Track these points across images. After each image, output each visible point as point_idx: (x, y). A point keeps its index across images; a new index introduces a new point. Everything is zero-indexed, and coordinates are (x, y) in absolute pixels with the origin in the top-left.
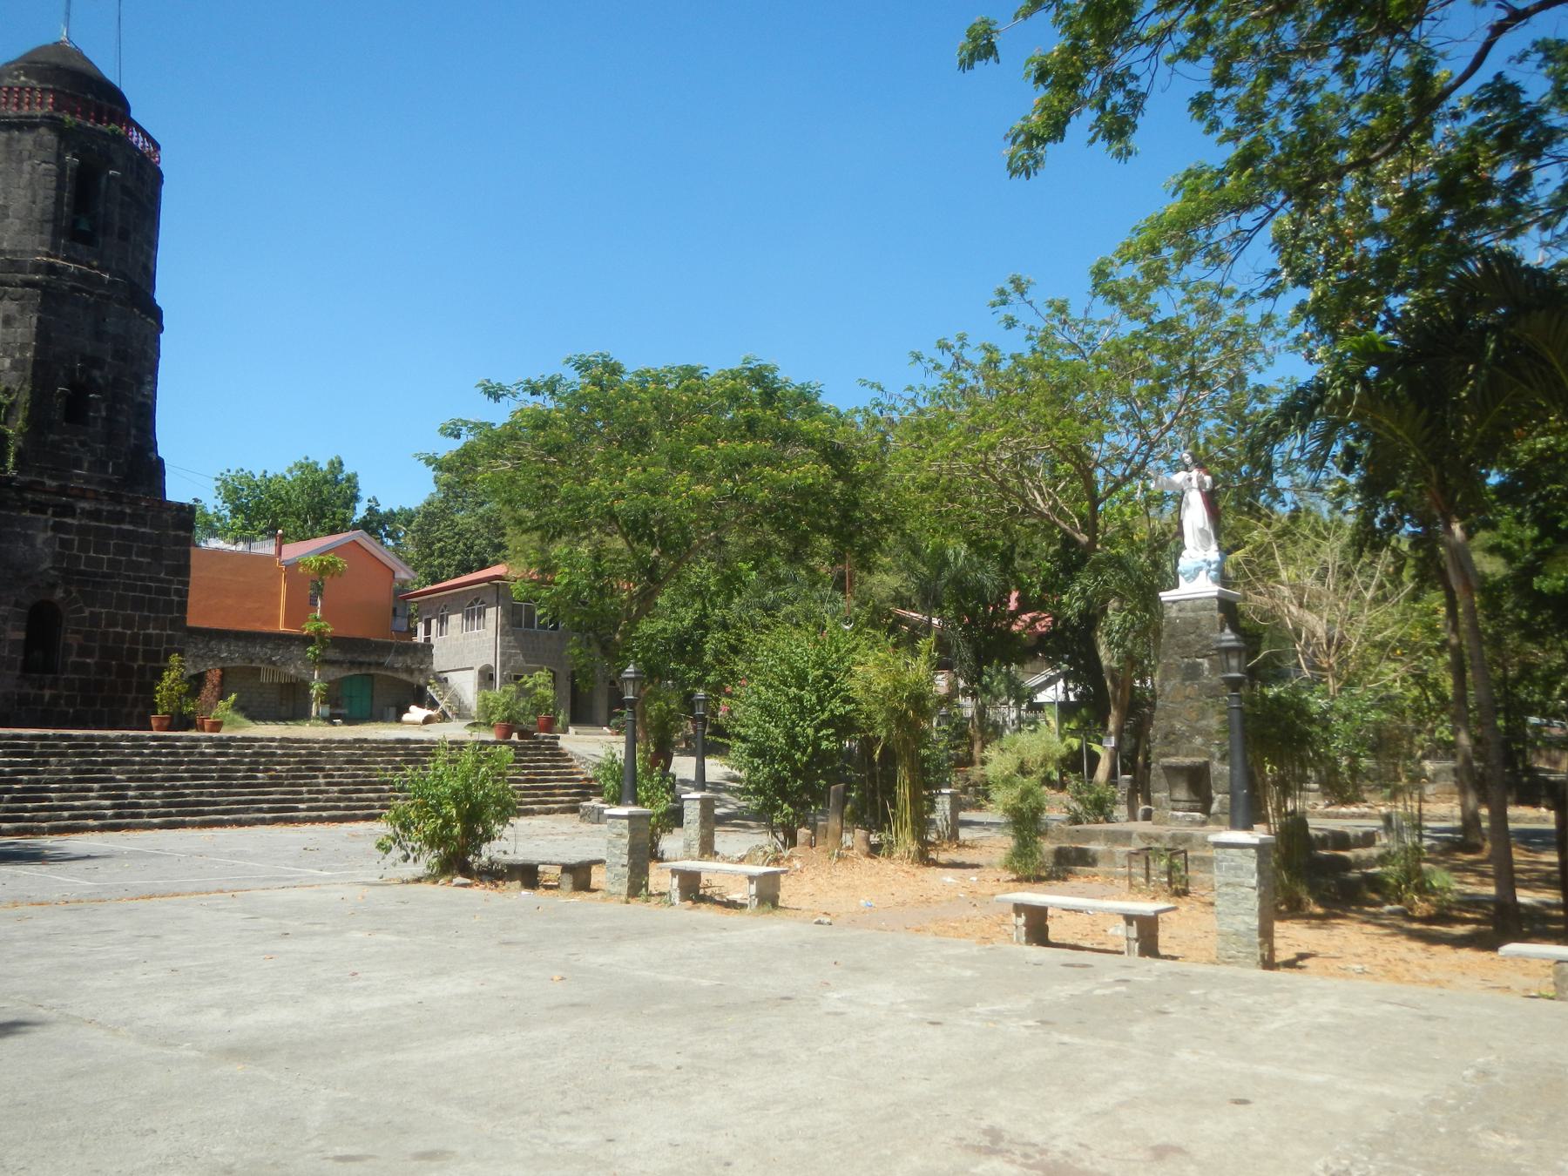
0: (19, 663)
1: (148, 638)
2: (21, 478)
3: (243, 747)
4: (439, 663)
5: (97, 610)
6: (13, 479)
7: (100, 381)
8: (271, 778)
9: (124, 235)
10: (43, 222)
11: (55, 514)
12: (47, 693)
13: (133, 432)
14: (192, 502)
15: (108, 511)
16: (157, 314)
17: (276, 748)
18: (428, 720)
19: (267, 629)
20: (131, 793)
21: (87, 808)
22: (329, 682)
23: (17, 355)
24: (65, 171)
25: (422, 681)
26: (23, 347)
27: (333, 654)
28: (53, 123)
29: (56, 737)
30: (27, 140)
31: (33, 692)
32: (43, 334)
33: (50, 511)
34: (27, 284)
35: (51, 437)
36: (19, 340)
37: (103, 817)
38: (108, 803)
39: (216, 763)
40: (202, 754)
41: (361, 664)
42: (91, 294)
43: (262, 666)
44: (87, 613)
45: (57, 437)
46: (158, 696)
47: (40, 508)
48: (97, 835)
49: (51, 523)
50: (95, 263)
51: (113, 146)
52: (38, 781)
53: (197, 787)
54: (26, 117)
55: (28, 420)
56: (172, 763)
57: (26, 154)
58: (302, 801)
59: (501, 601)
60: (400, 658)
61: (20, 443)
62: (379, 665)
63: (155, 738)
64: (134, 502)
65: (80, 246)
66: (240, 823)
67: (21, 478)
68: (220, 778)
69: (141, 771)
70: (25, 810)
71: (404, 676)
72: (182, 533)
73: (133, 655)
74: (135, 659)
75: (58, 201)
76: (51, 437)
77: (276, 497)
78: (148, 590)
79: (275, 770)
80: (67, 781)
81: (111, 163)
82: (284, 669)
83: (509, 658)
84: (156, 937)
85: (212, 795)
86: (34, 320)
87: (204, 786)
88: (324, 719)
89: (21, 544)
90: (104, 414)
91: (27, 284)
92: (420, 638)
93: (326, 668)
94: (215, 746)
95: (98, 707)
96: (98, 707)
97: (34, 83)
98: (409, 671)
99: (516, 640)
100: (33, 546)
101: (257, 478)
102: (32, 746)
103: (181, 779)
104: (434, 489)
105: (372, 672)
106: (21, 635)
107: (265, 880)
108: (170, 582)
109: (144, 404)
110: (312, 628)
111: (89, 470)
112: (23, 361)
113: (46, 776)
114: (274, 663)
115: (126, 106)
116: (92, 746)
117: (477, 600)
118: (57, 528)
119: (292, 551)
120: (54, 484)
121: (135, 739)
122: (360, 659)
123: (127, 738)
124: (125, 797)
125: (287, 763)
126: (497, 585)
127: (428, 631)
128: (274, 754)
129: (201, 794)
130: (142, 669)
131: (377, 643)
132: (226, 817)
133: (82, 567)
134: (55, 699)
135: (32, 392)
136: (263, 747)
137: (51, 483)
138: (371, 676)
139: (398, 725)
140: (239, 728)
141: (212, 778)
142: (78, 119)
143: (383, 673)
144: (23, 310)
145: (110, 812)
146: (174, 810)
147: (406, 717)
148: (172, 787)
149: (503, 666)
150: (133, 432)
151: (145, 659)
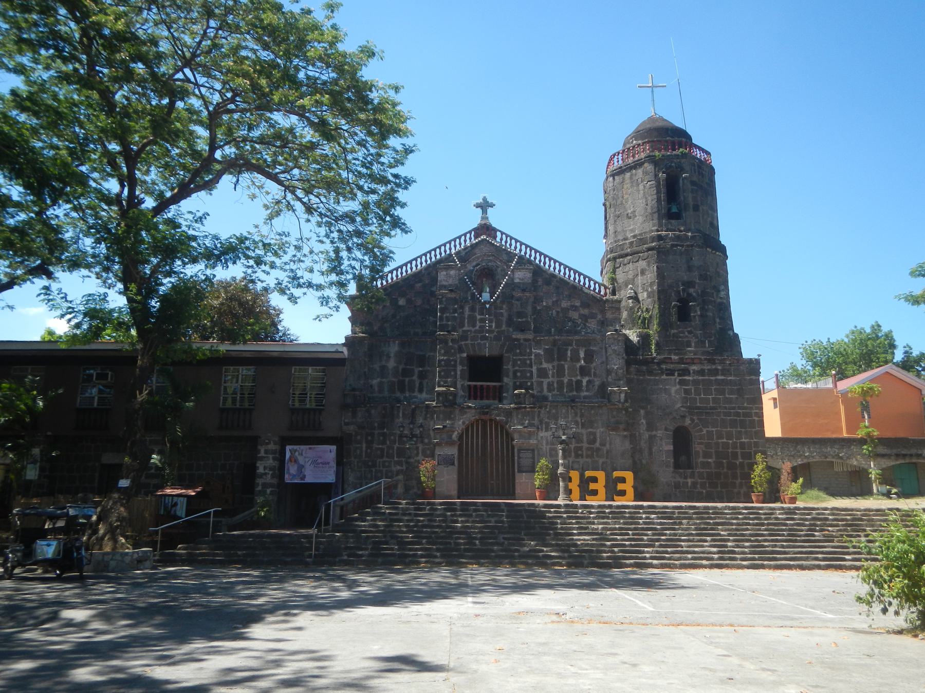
0: (672, 465)
1: (742, 444)
2: (659, 357)
3: (804, 514)
5: (710, 429)
6: (654, 358)
7: (694, 294)
8: (824, 536)
9: (696, 208)
10: (652, 214)
11: (679, 375)
12: (689, 481)
13: (718, 320)
14: (757, 357)
15: (708, 370)
16: (723, 249)
17: (829, 514)
19: (834, 436)
20: (729, 544)
21: (703, 552)
22: (882, 470)
23: (650, 290)
24: (660, 184)
26: (651, 284)
27: (881, 450)
28: (651, 159)
29: (687, 507)
30: (640, 172)
31: (681, 480)
32: (661, 275)
33: (676, 374)
34: (649, 249)
35: (673, 331)
36: (649, 281)
37: (712, 559)
38: (715, 550)
39: (786, 525)
40: (777, 519)
41: (904, 456)
42: (682, 246)
44: (705, 432)
45: (676, 331)
46: (753, 481)
47: (671, 373)
48: (707, 570)
49: (678, 380)
50: (682, 229)
51: (683, 161)
52: (675, 535)
53: (772, 541)
54: (638, 161)
55: (659, 324)
56: (757, 524)
57: (640, 180)
58: (848, 554)
61: (657, 338)
63: (746, 508)
64: (722, 362)
65: (673, 221)
66: (802, 568)
67: (659, 357)
68: (789, 535)
69: (737, 530)
70: (667, 552)
72: (754, 377)
73: (735, 455)
74: (737, 458)
75: (659, 200)
76: (673, 331)
77: (837, 353)
78: (738, 414)
79: (828, 531)
80: (692, 535)
81: (683, 170)
84: (634, 665)
85: (783, 547)
86: (655, 268)
87: (777, 541)
88: (883, 495)
89: (664, 395)
90: (699, 313)
91: (649, 249)
93: (879, 459)
94: (786, 513)
95: (719, 489)
96: (719, 489)
97: (640, 142)
100: (670, 395)
101: (825, 344)
102: (673, 513)
103: (762, 535)
105: (914, 461)
106: (671, 447)
107: (775, 618)
108: (751, 408)
109: (721, 304)
110: (863, 433)
111: (695, 347)
112: (653, 292)
113: (680, 532)
114: (841, 458)
115: (689, 138)
116: (708, 513)
118: (682, 383)
119: (843, 385)
120: (676, 358)
121: (734, 508)
122: (903, 452)
123: (729, 508)
124: (726, 546)
125: (837, 526)
128: (827, 519)
129: (775, 546)
130: (742, 464)
131: (913, 440)
132: (792, 563)
133: (698, 405)
134: (694, 485)
135: (659, 308)
136: (818, 514)
137: (675, 357)
140: (822, 501)
141: (783, 535)
142: (663, 152)
144: (649, 265)
145: (716, 556)
146: (756, 556)
148: (757, 541)
150: (718, 320)
151: (742, 458)
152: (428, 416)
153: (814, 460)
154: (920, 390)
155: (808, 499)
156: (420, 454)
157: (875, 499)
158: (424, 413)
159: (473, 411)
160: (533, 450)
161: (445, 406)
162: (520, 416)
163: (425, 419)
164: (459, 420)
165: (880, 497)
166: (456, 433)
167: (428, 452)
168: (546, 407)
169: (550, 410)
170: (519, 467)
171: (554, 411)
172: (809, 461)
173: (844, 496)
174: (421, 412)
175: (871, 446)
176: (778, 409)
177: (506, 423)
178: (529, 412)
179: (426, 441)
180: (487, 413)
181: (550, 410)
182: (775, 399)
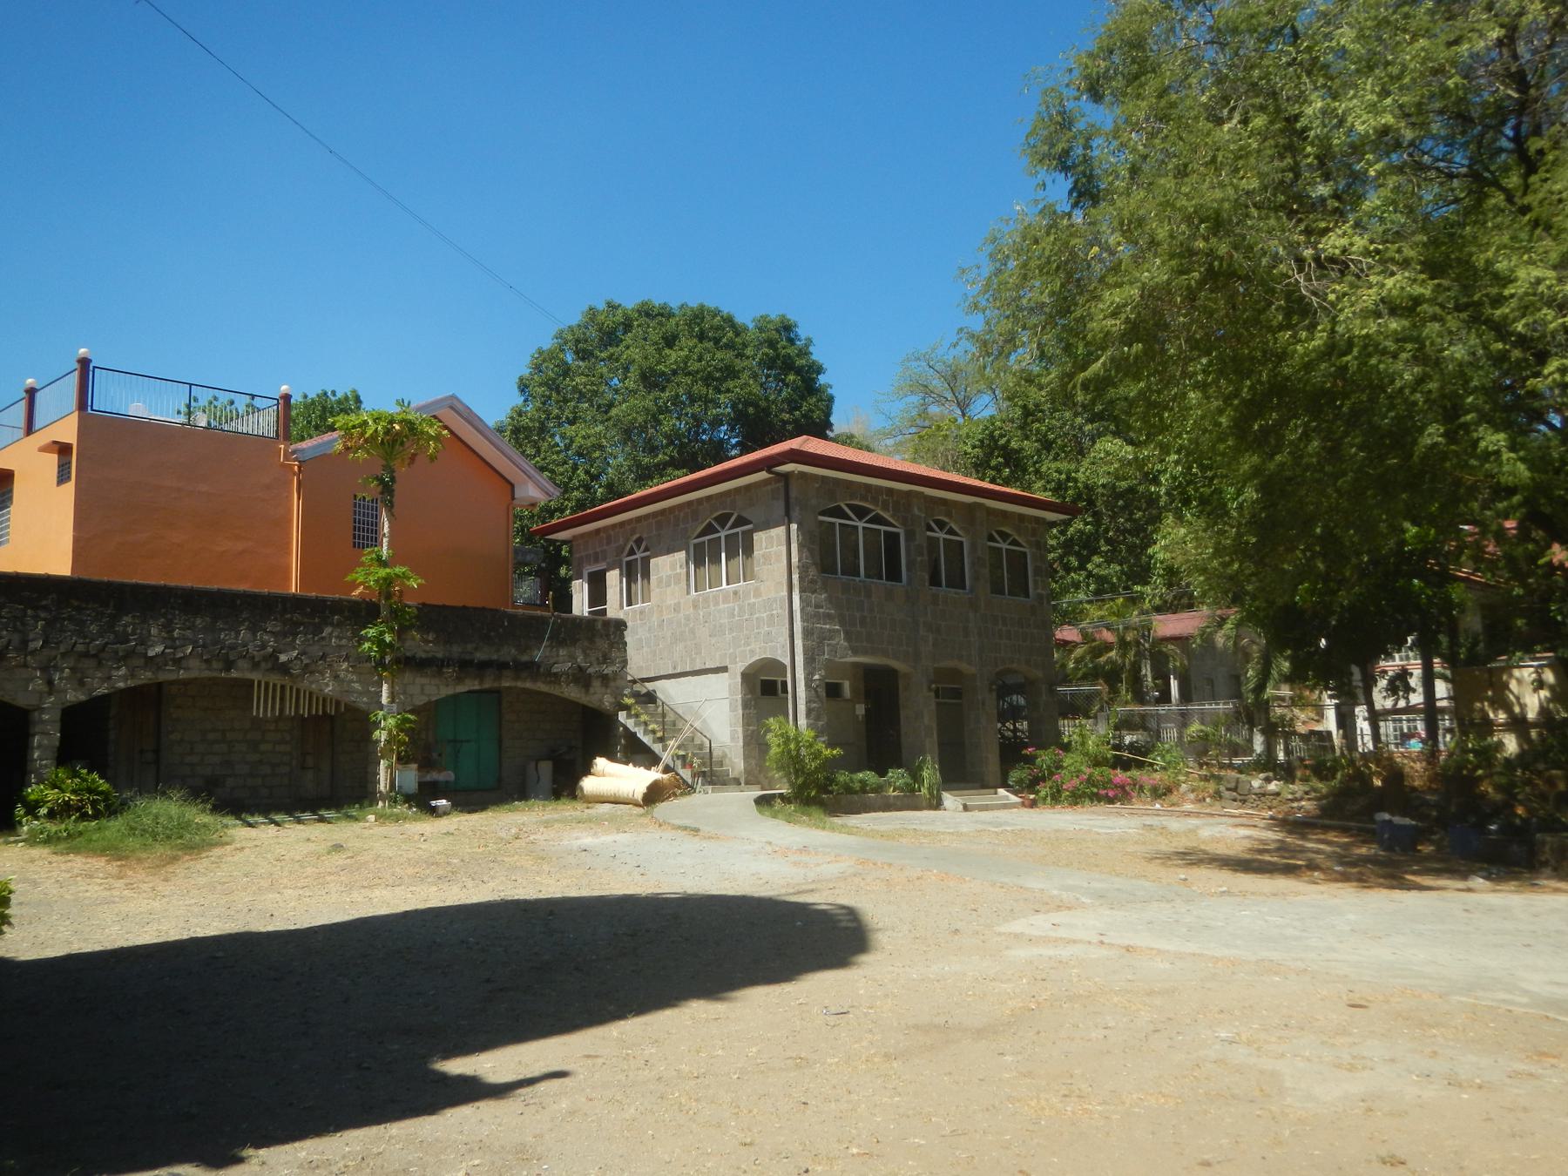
4: (639, 659)
18: (654, 795)
25: (608, 702)
27: (419, 644)
41: (484, 666)
43: (255, 676)
59: (796, 513)
60: (562, 652)
62: (531, 668)
71: (572, 692)
82: (307, 684)
83: (822, 639)
88: (409, 799)
92: (581, 604)
93: (408, 676)
98: (582, 678)
99: (830, 599)
104: (519, 400)
114: (284, 669)
117: (723, 520)
122: (480, 656)
126: (786, 477)
127: (598, 595)
138: (497, 692)
139: (566, 810)
143: (528, 685)
147: (589, 784)
149: (810, 660)
153: (182, 674)
154: (512, 486)
155: (131, 842)
157: (381, 817)
165: (400, 809)
172: (163, 677)
173: (280, 808)
175: (391, 630)
176: (70, 487)
182: (63, 450)
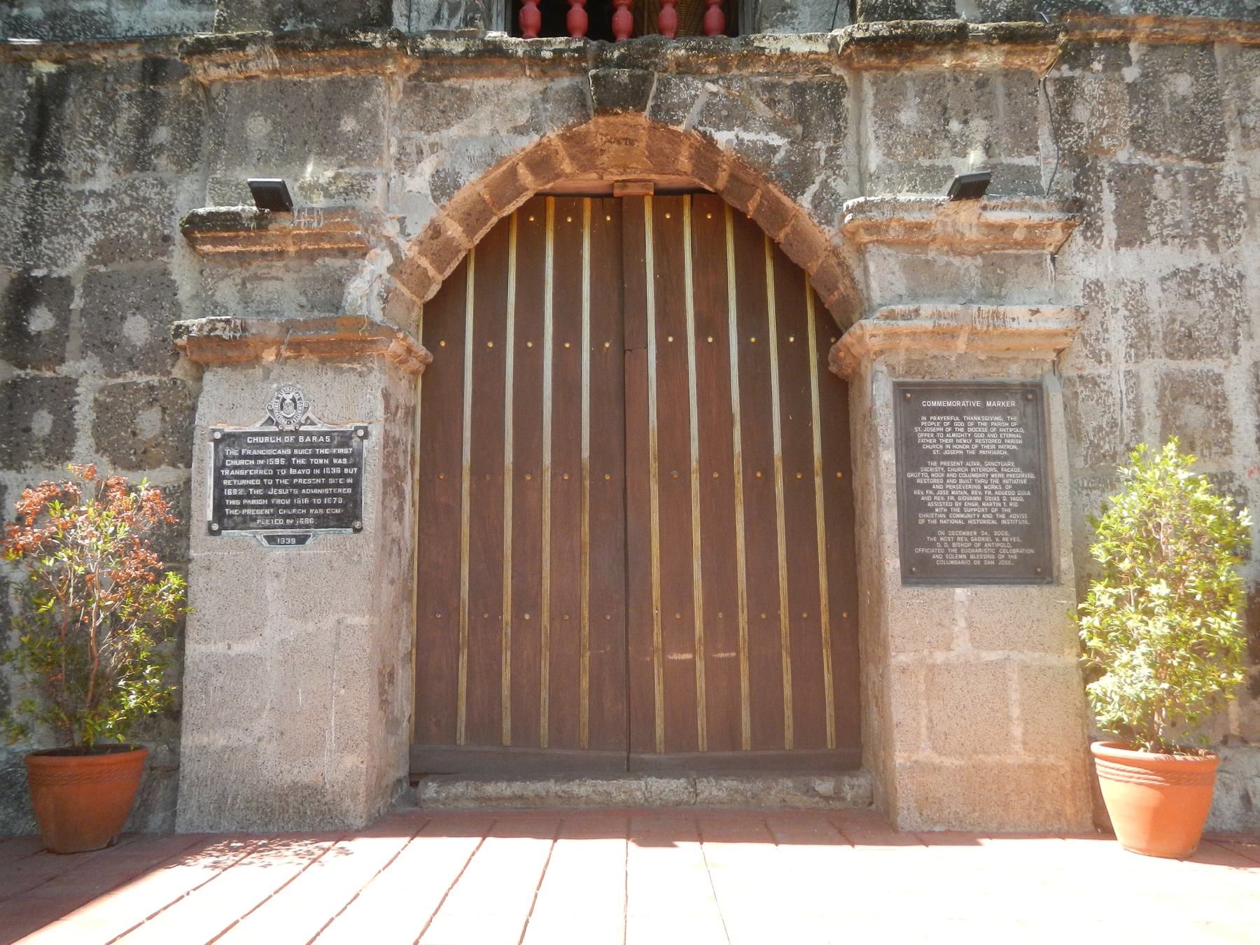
152: (162, 134)
156: (84, 443)
158: (128, 113)
159: (525, 87)
160: (1032, 393)
161: (285, 45)
162: (908, 116)
163: (138, 160)
164: (404, 162)
166: (379, 261)
167: (150, 422)
168: (1117, 50)
169: (1151, 78)
170: (911, 533)
171: (1182, 84)
174: (108, 110)
177: (798, 177)
178: (982, 84)
179: (137, 330)
180: (635, 97)
181: (1151, 78)
